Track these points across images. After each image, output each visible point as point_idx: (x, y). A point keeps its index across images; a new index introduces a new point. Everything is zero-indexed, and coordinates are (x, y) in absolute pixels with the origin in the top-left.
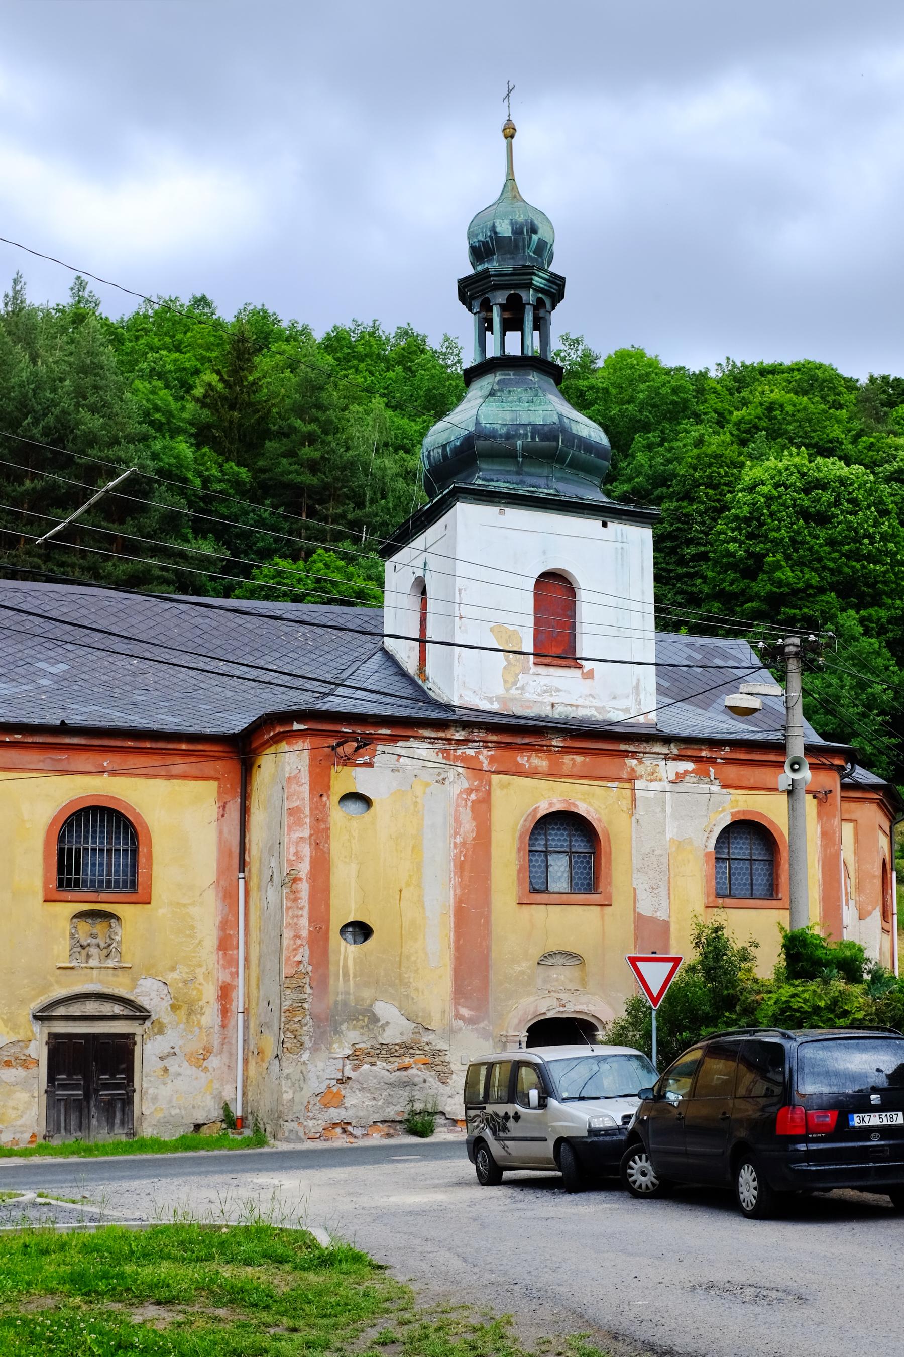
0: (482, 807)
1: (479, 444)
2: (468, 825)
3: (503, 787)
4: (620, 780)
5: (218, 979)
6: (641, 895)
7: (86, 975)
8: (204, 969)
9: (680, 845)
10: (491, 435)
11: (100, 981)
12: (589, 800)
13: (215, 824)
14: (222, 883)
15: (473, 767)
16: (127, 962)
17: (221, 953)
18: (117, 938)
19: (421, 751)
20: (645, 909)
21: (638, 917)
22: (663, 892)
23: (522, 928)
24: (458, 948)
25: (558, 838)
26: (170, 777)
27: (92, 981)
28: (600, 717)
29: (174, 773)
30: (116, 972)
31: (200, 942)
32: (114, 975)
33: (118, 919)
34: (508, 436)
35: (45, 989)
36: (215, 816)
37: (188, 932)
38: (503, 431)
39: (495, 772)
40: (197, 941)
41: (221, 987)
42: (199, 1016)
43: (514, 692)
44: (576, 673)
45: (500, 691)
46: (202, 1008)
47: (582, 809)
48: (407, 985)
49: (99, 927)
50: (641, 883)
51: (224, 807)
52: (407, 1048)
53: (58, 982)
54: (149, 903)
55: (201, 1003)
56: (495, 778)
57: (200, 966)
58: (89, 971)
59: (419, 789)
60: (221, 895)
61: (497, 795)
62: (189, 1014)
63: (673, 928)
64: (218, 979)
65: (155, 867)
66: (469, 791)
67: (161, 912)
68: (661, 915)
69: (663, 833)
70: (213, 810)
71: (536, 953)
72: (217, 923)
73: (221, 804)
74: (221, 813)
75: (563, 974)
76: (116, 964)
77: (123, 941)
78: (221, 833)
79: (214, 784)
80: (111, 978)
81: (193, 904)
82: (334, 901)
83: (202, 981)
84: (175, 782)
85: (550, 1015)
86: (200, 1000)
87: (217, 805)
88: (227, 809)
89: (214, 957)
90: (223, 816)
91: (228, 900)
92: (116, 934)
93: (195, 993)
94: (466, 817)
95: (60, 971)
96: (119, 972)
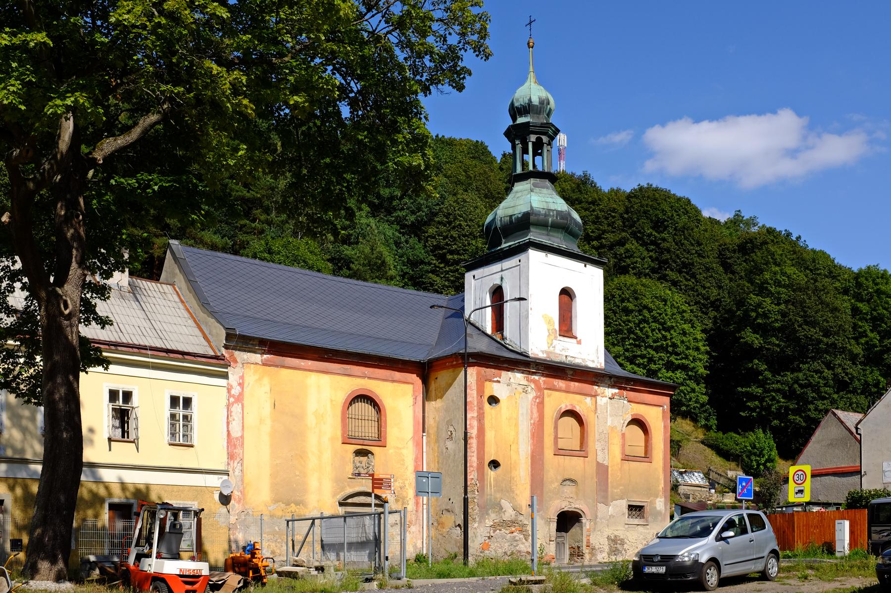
0: (541, 405)
1: (532, 218)
2: (536, 415)
3: (549, 396)
4: (591, 396)
6: (599, 453)
9: (613, 428)
10: (538, 214)
12: (582, 404)
15: (539, 389)
19: (518, 377)
20: (600, 460)
21: (598, 463)
22: (606, 451)
23: (555, 467)
24: (532, 475)
25: (571, 421)
28: (583, 364)
34: (545, 215)
35: (343, 489)
38: (543, 212)
39: (546, 389)
43: (551, 349)
44: (574, 341)
45: (545, 348)
47: (578, 409)
48: (513, 492)
49: (364, 459)
50: (598, 446)
52: (513, 522)
56: (546, 392)
59: (517, 395)
61: (546, 399)
63: (610, 469)
66: (536, 397)
68: (606, 463)
69: (606, 423)
70: (410, 400)
71: (560, 479)
75: (569, 489)
79: (409, 388)
82: (486, 450)
85: (566, 509)
94: (535, 411)
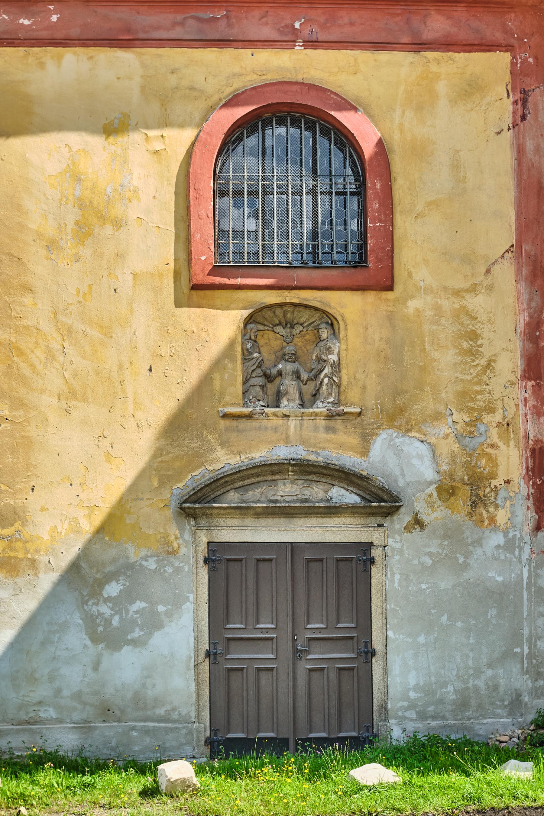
5: (527, 437)
7: (275, 429)
8: (498, 417)
11: (303, 442)
13: (508, 135)
14: (526, 247)
16: (353, 405)
17: (530, 384)
18: (333, 358)
26: (419, 46)
27: (287, 442)
29: (427, 35)
30: (332, 423)
31: (489, 365)
32: (328, 429)
33: (331, 323)
36: (509, 120)
37: (465, 345)
40: (483, 362)
41: (533, 451)
42: (491, 509)
46: (496, 490)
51: (525, 102)
53: (222, 444)
54: (390, 288)
55: (494, 483)
57: (492, 410)
58: (280, 422)
60: (525, 271)
62: (474, 505)
64: (527, 437)
65: (398, 219)
67: (412, 305)
72: (521, 327)
73: (518, 96)
74: (520, 113)
76: (331, 407)
77: (343, 362)
78: (520, 151)
80: (322, 435)
81: (474, 289)
83: (496, 439)
84: (430, 55)
86: (493, 476)
87: (511, 99)
88: (530, 105)
89: (518, 393)
90: (523, 118)
91: (539, 282)
92: (329, 350)
93: (483, 463)
95: (223, 423)
96: (338, 423)
